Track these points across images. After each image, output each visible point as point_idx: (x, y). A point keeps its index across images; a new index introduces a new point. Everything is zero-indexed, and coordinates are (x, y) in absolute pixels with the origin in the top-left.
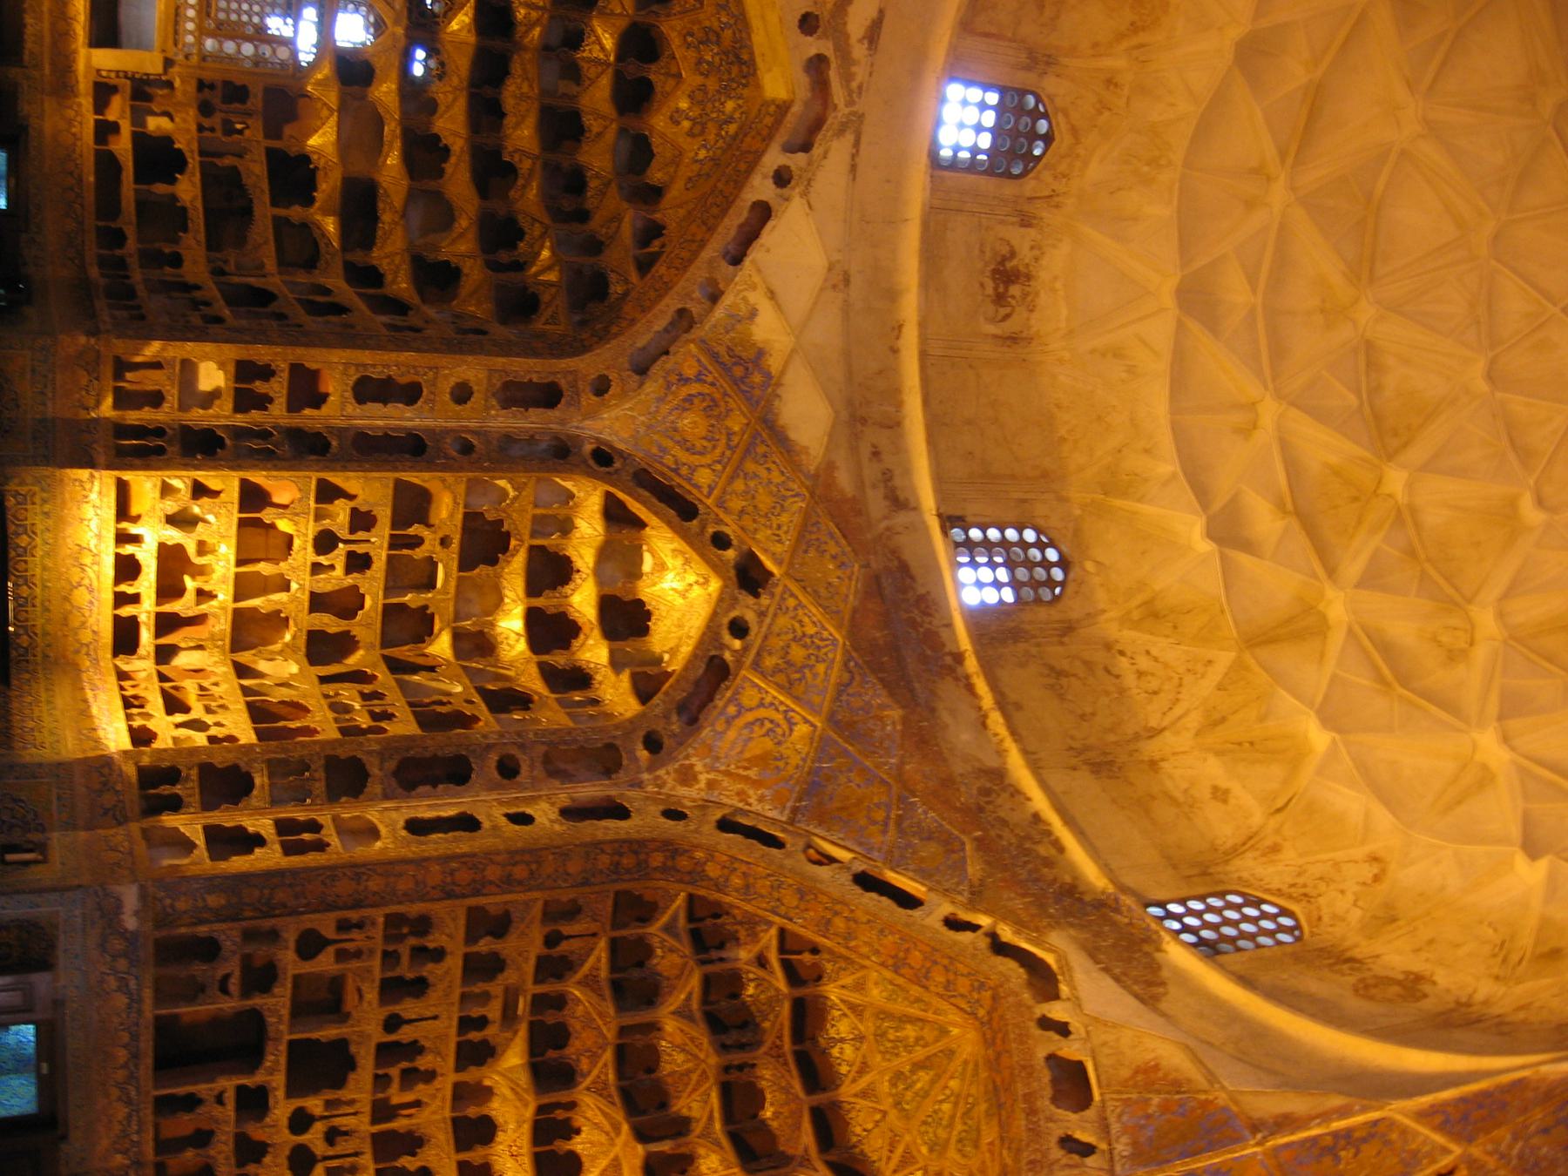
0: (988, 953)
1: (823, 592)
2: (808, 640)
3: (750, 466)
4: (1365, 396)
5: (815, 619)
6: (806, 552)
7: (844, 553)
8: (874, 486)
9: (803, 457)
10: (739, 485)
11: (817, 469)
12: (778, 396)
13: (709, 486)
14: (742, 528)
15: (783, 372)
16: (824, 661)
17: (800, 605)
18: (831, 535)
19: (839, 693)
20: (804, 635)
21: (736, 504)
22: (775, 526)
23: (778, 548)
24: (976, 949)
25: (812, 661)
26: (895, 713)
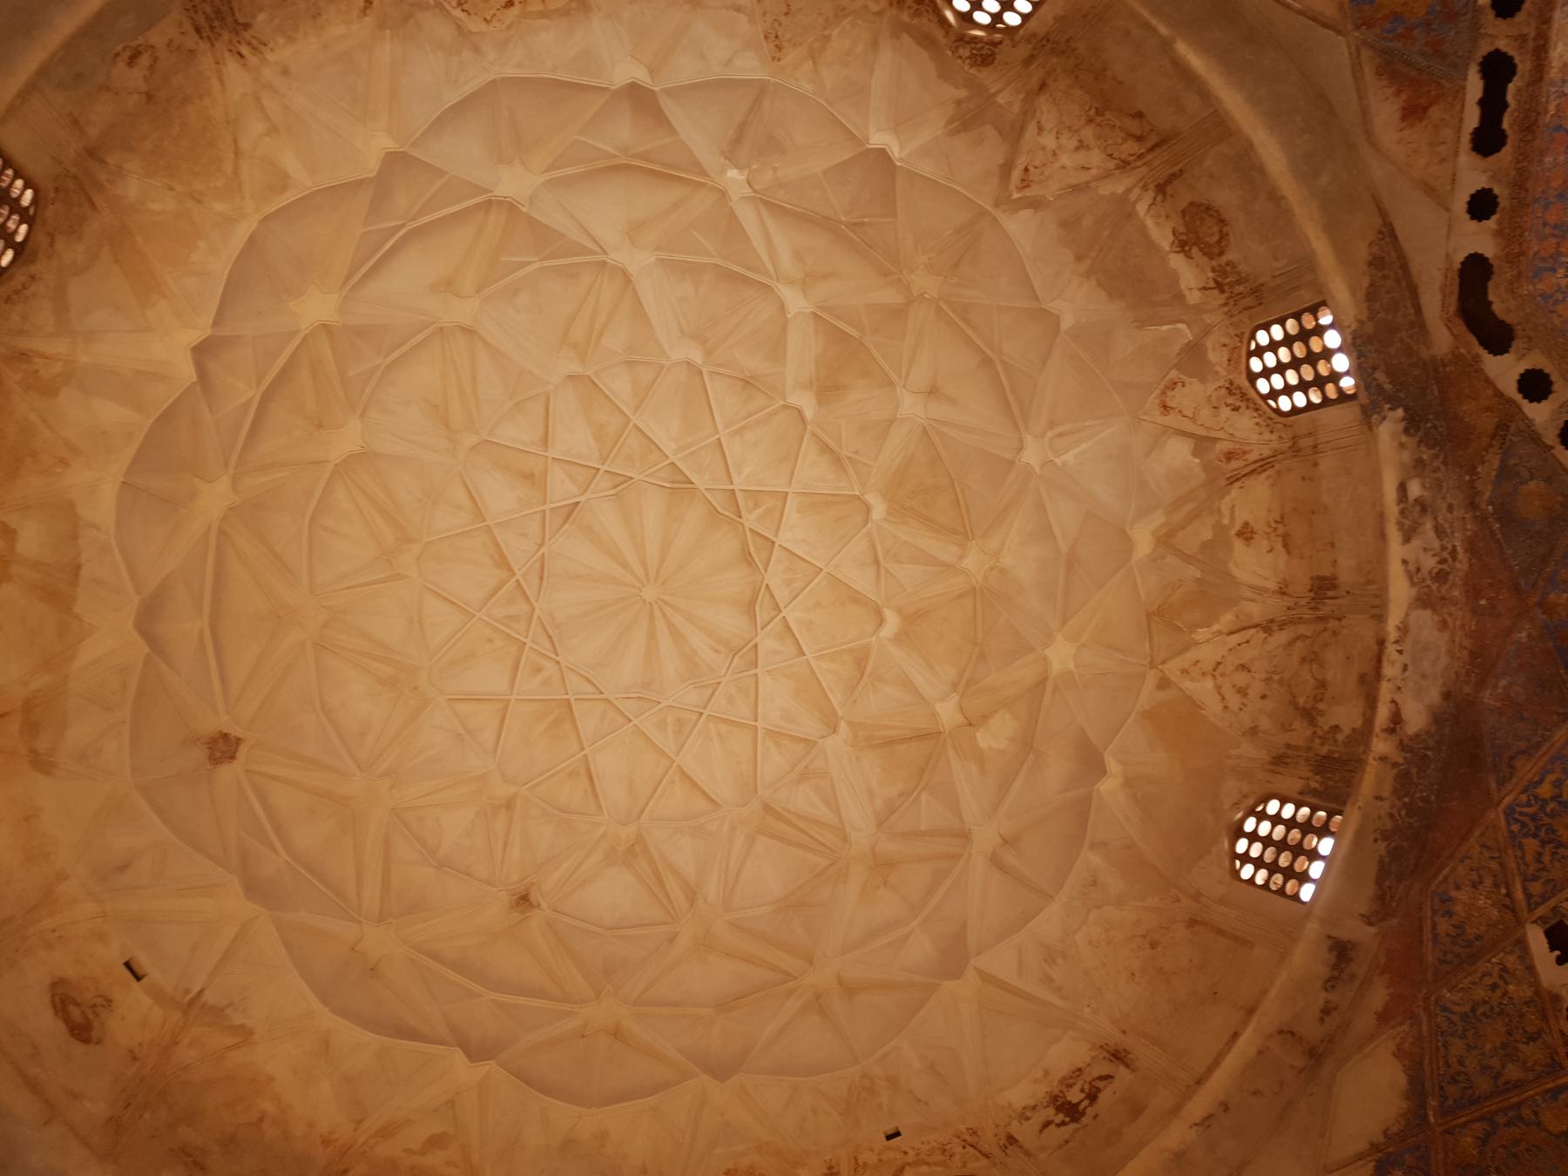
0: (1518, 330)
1: (1488, 882)
2: (1542, 833)
3: (1484, 1085)
4: (916, 793)
5: (1519, 853)
6: (1478, 938)
7: (1434, 912)
8: (1353, 977)
9: (1407, 1046)
10: (1513, 1072)
11: (1401, 1024)
12: (1385, 1133)
13: (1555, 1098)
14: (1544, 1017)
15: (1360, 1157)
16: (1536, 798)
17: (1525, 880)
18: (1435, 938)
19: (1538, 745)
20: (1544, 843)
21: (1532, 1052)
22: (1499, 992)
23: (1511, 961)
24: (1529, 338)
25: (1551, 806)
26: (1488, 698)
